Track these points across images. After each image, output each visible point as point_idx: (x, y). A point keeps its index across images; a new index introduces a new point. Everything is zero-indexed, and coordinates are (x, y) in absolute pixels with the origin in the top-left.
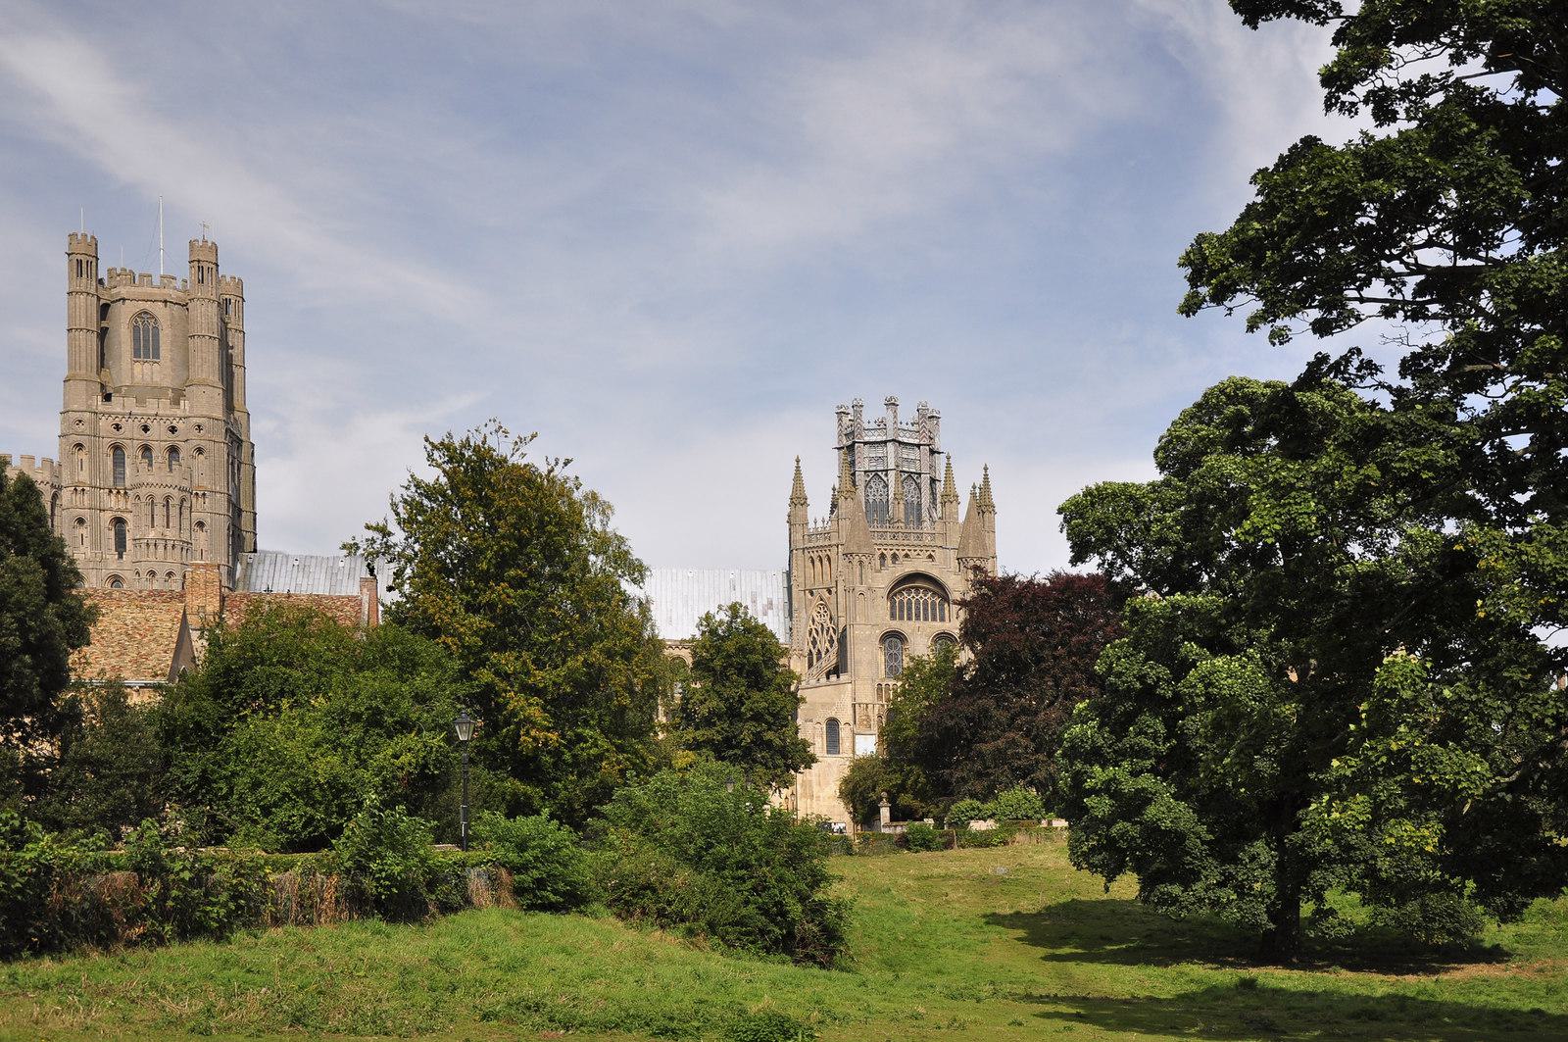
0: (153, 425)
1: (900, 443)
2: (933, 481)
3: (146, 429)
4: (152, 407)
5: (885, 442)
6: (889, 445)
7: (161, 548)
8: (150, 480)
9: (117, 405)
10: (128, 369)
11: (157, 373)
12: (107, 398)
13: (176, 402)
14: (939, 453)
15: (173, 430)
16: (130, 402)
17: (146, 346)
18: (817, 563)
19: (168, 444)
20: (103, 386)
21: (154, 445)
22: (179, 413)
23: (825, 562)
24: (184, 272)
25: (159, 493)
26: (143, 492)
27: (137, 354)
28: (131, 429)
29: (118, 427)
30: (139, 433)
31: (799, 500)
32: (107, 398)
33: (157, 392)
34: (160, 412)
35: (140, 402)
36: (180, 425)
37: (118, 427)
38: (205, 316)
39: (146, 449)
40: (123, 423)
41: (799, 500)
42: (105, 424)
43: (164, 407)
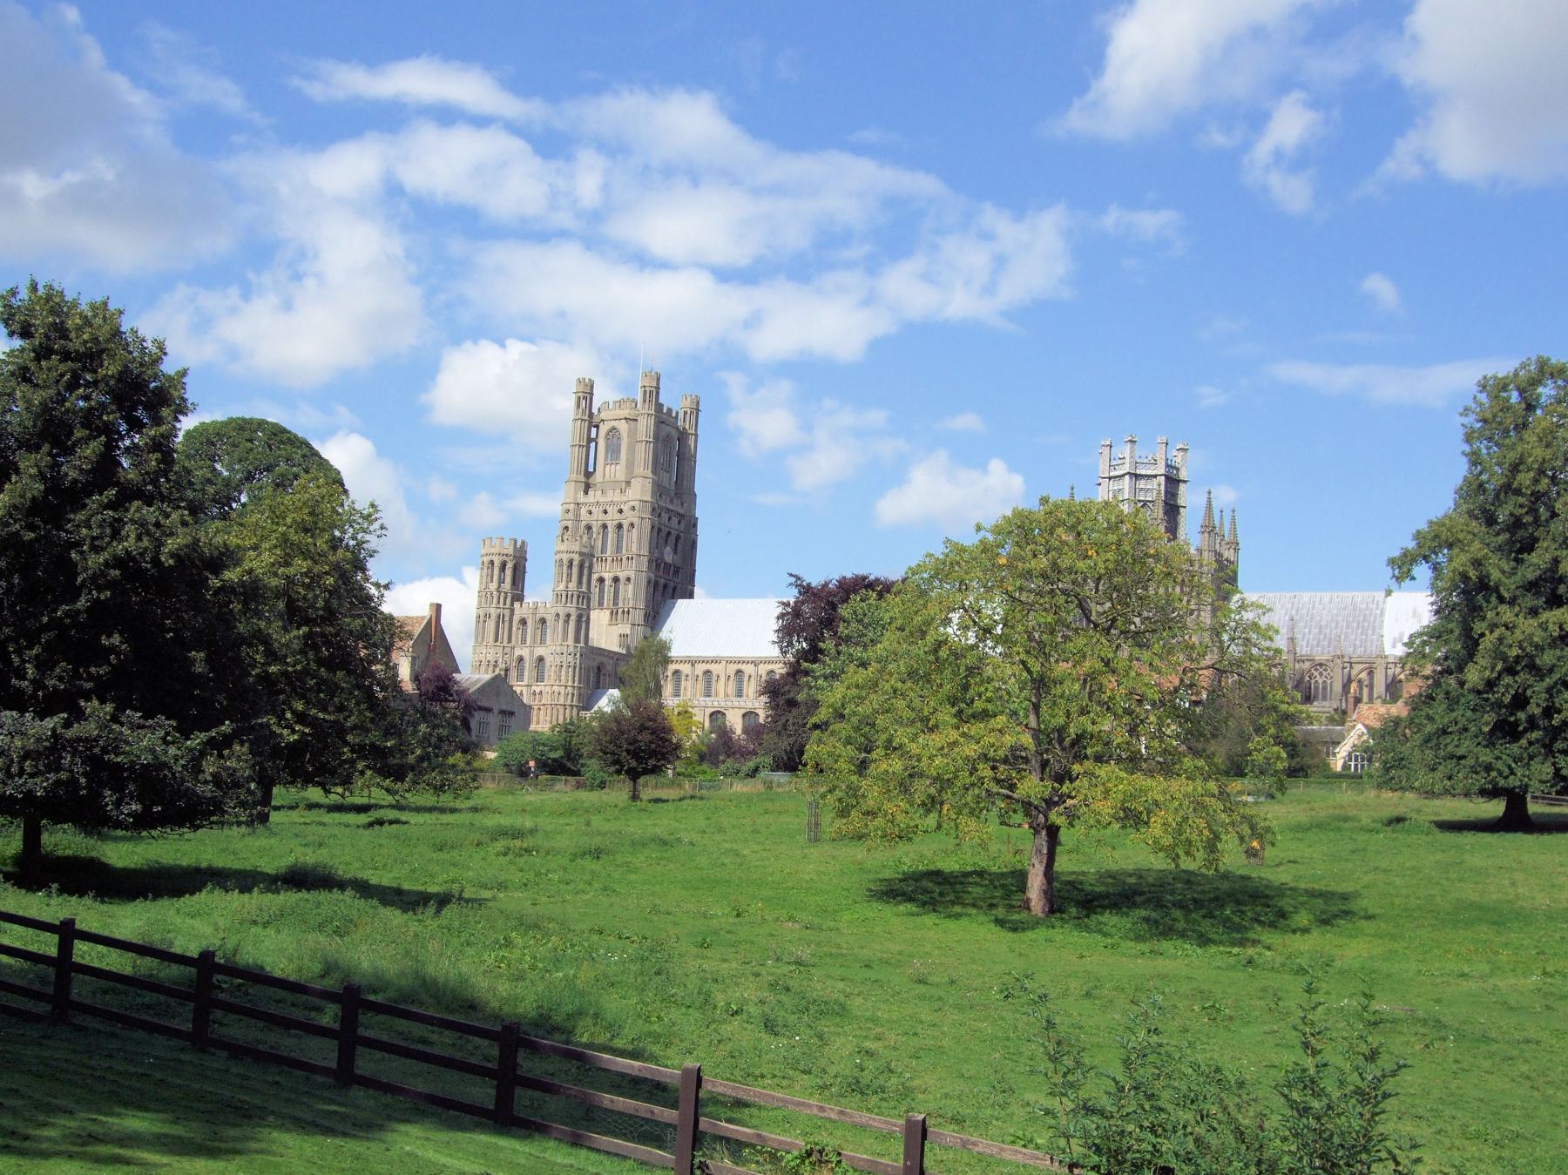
0: (610, 510)
1: (1115, 477)
3: (606, 512)
6: (1127, 477)
7: (564, 596)
11: (618, 472)
14: (1185, 482)
15: (621, 511)
19: (617, 522)
21: (609, 524)
22: (625, 499)
29: (590, 513)
34: (615, 499)
36: (625, 508)
37: (590, 513)
39: (605, 527)
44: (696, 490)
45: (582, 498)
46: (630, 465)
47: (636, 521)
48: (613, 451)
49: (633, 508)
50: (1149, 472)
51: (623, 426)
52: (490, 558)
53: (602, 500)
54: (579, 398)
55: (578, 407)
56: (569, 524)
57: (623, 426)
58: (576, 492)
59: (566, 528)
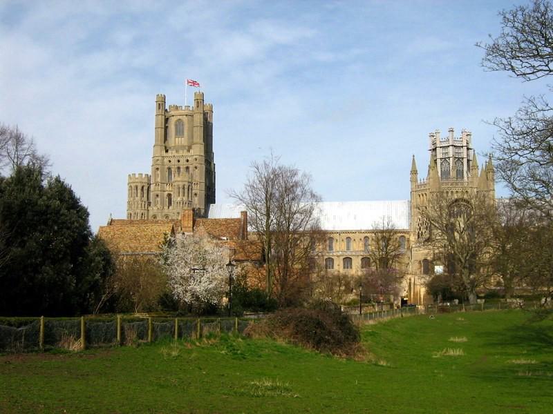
0: (181, 160)
2: (468, 161)
3: (179, 161)
4: (181, 153)
5: (449, 146)
8: (179, 179)
9: (170, 153)
10: (173, 140)
11: (183, 141)
12: (167, 151)
13: (189, 151)
15: (188, 161)
16: (174, 152)
17: (179, 132)
18: (421, 196)
20: (166, 147)
23: (425, 195)
24: (193, 104)
25: (181, 184)
26: (176, 184)
27: (176, 134)
28: (174, 161)
29: (170, 161)
30: (177, 163)
31: (414, 172)
32: (167, 151)
33: (183, 147)
35: (177, 151)
38: (199, 119)
40: (171, 159)
41: (414, 172)
42: (166, 160)
43: (185, 153)
44: (214, 151)
45: (165, 154)
46: (191, 136)
47: (198, 166)
48: (179, 132)
49: (196, 159)
50: (459, 145)
51: (185, 119)
52: (135, 184)
53: (176, 155)
54: (159, 104)
55: (159, 108)
56: (159, 167)
57: (185, 119)
58: (161, 152)
59: (157, 169)
